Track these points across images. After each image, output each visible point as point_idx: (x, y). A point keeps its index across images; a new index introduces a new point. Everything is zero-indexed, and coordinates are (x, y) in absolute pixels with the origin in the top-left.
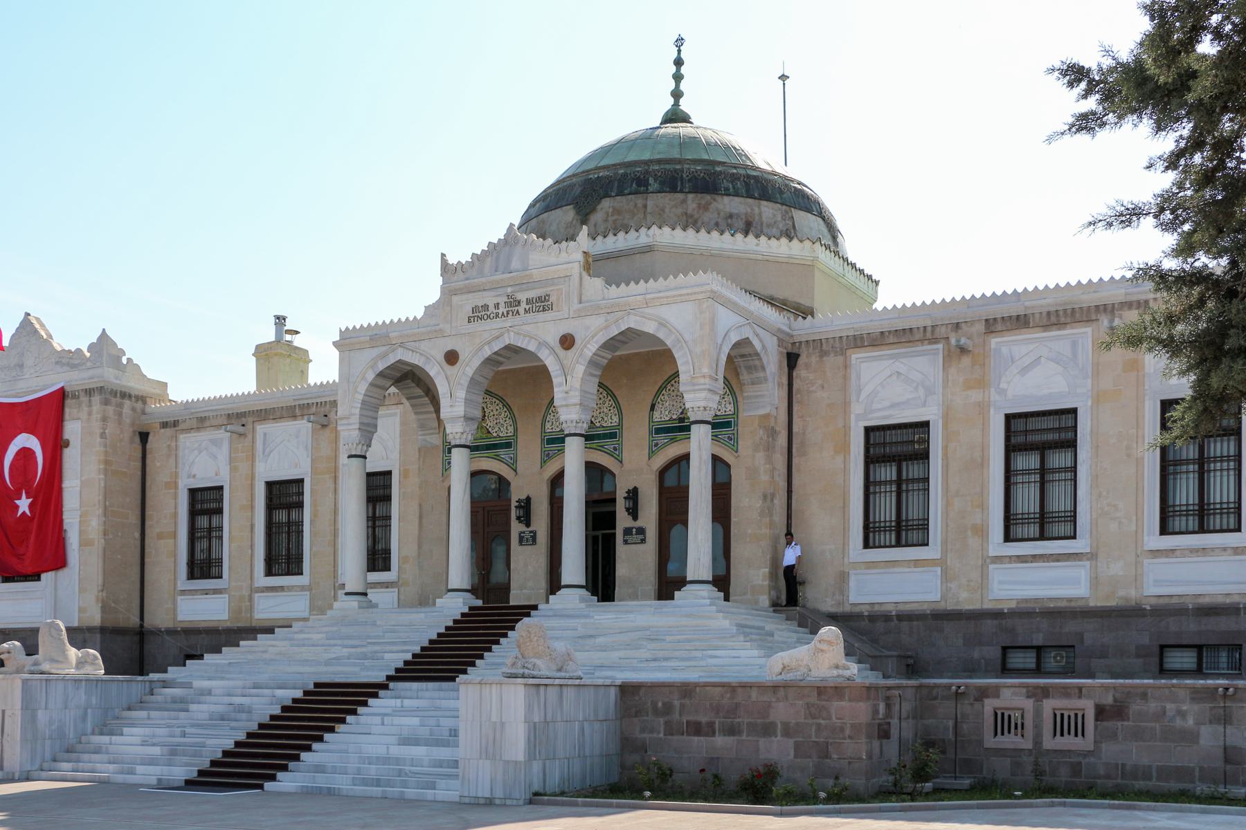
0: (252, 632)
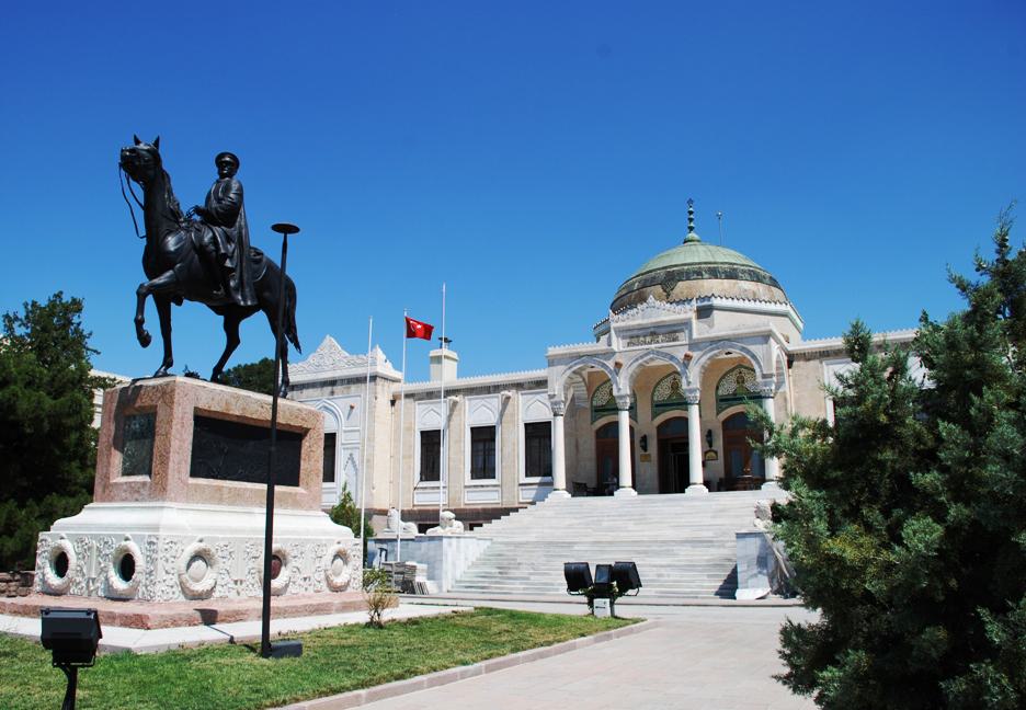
0: (506, 511)
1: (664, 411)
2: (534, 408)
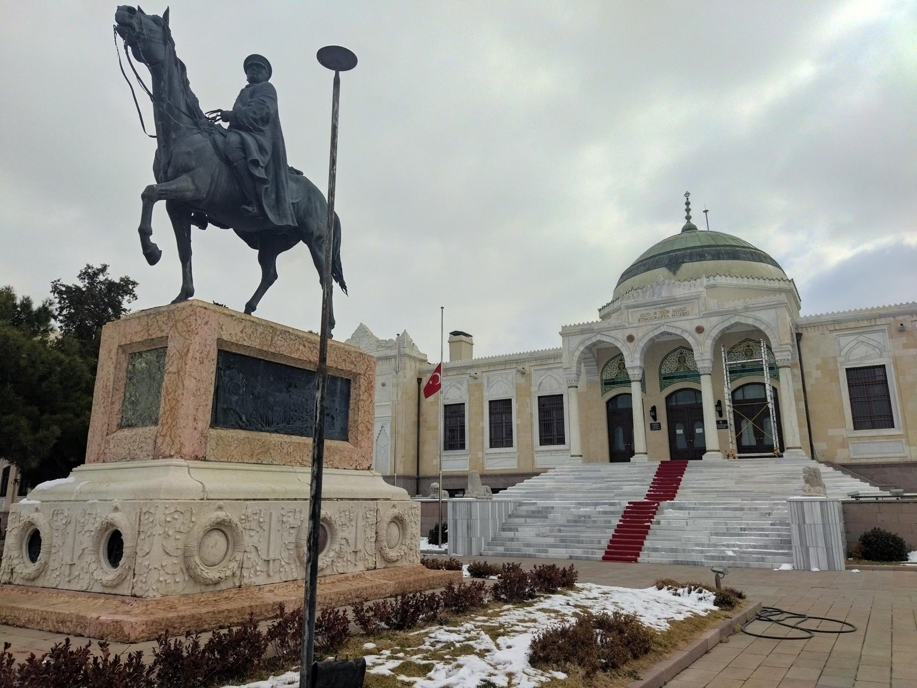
1: (671, 383)
2: (550, 383)
